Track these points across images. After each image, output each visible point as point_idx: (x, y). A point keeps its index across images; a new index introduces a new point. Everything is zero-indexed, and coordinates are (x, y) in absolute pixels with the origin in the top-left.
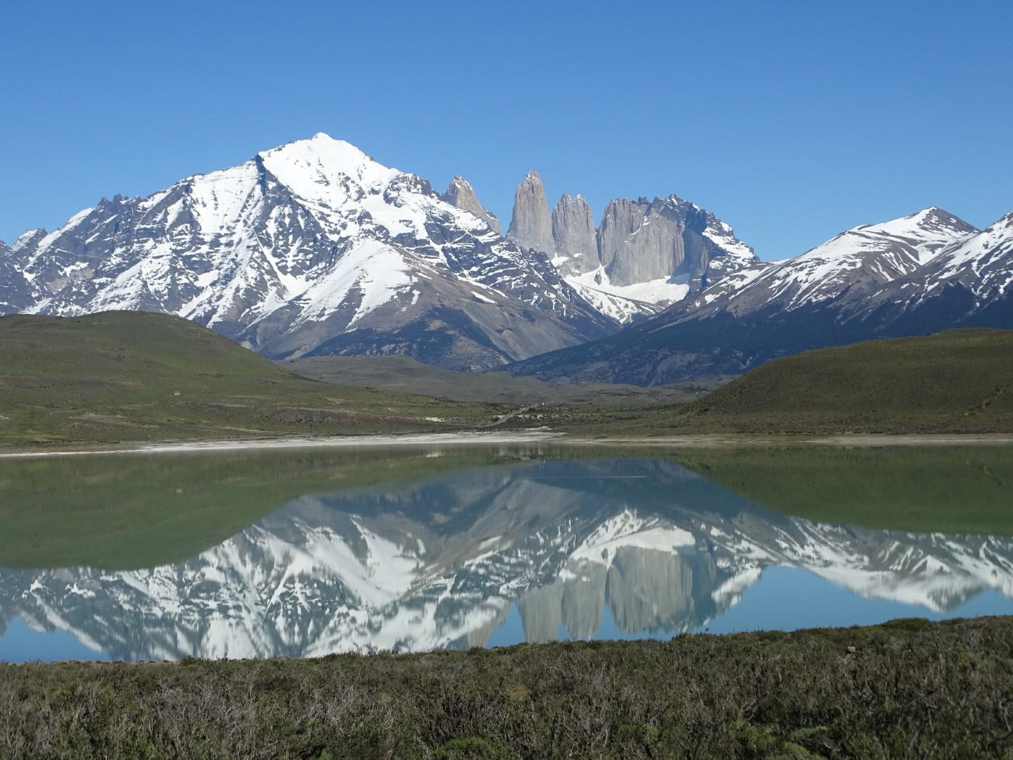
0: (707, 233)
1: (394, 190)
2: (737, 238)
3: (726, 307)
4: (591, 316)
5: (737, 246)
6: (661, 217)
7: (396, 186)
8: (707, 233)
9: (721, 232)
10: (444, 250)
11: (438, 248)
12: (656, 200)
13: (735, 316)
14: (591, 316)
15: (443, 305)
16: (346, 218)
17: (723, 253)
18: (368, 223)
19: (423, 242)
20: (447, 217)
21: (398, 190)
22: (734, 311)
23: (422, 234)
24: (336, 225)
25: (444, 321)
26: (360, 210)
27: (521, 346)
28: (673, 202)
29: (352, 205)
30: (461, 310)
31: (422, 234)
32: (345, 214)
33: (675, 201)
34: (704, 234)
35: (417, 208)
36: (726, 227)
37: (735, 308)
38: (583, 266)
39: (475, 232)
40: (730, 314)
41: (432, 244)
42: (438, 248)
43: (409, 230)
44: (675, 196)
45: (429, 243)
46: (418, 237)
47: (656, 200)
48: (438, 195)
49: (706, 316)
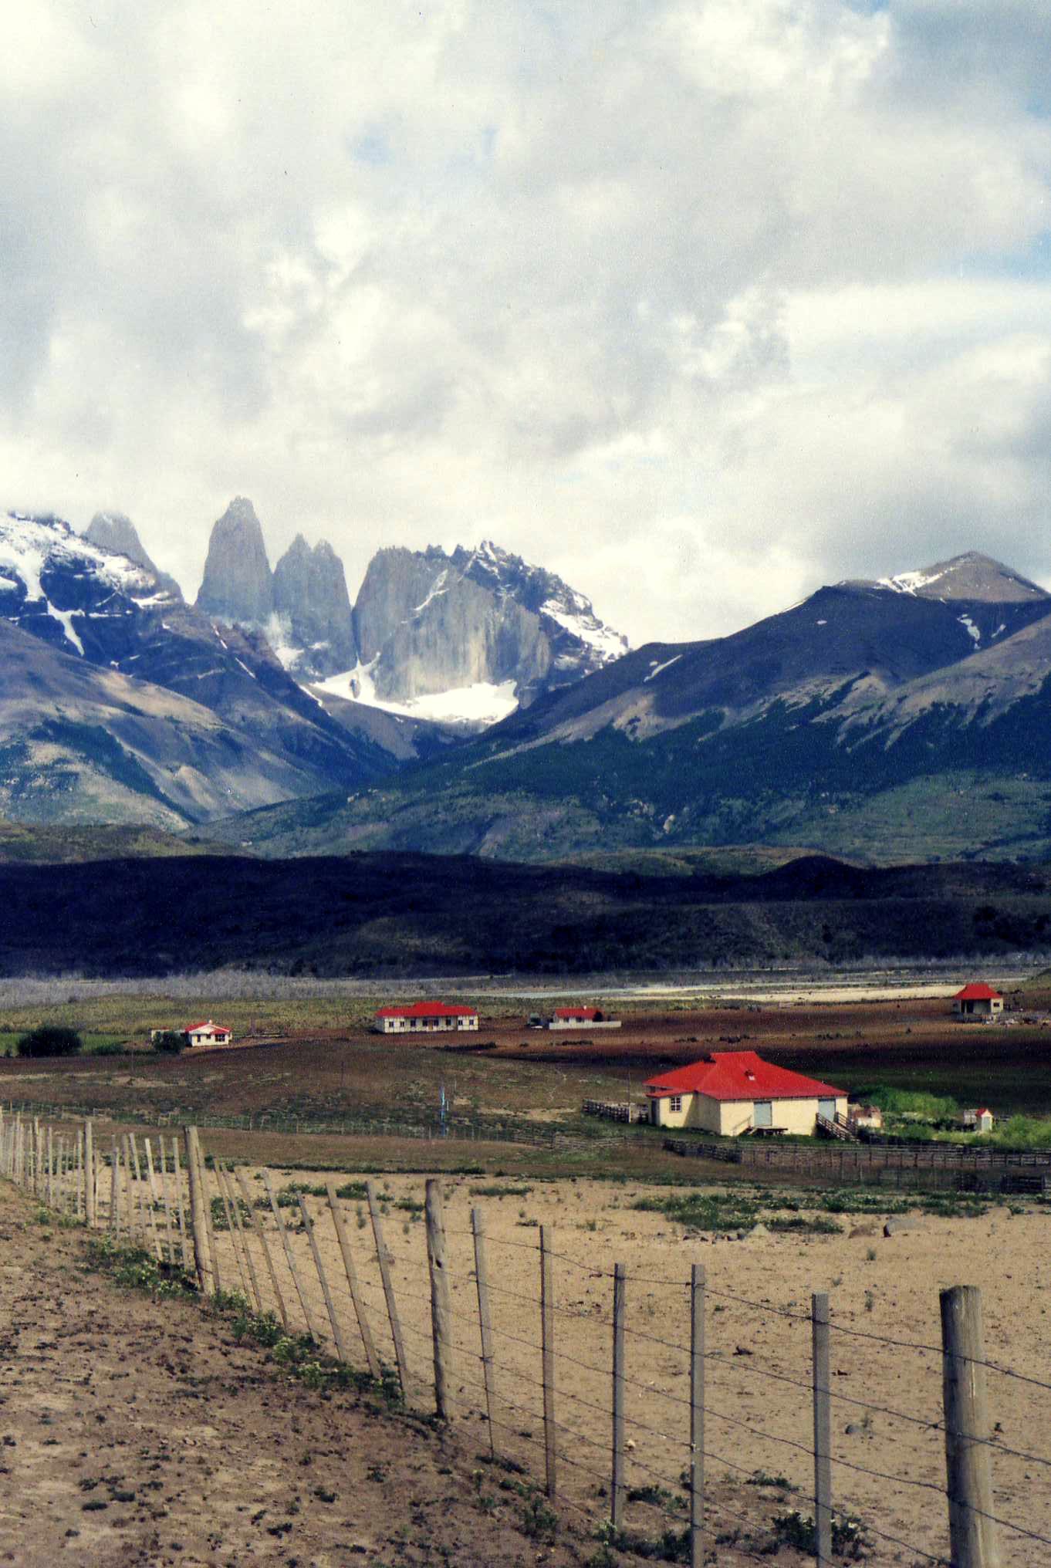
0: (551, 608)
2: (598, 617)
3: (613, 721)
4: (343, 745)
5: (598, 632)
6: (466, 581)
8: (551, 608)
9: (571, 610)
10: (75, 621)
11: (63, 616)
12: (459, 552)
13: (631, 738)
14: (343, 745)
15: (62, 718)
17: (577, 642)
19: (41, 606)
20: (79, 565)
22: (630, 728)
23: (35, 593)
25: (66, 744)
27: (212, 796)
28: (487, 555)
30: (100, 727)
31: (35, 593)
33: (490, 552)
34: (542, 610)
35: (24, 544)
36: (580, 603)
37: (631, 722)
38: (328, 665)
39: (132, 590)
40: (620, 735)
41: (52, 611)
42: (63, 616)
43: (11, 585)
44: (491, 544)
45: (45, 609)
46: (27, 599)
47: (459, 552)
48: (66, 526)
49: (571, 739)
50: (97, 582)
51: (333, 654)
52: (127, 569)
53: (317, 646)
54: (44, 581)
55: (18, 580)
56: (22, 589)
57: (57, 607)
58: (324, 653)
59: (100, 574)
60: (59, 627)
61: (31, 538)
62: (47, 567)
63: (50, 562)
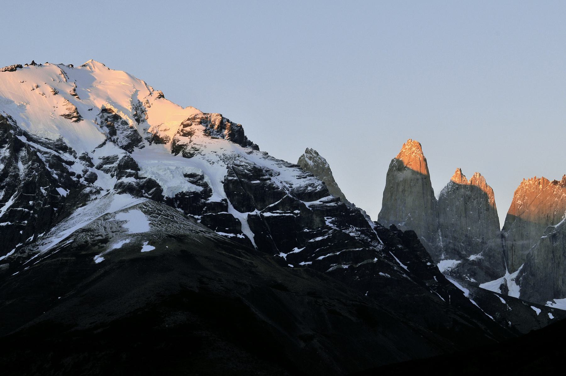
1: (185, 135)
7: (188, 129)
10: (251, 219)
11: (242, 217)
16: (99, 167)
18: (130, 175)
19: (221, 206)
21: (189, 134)
23: (218, 195)
24: (79, 177)
26: (121, 156)
29: (111, 150)
31: (218, 195)
32: (97, 162)
35: (214, 158)
42: (242, 217)
45: (226, 208)
50: (271, 187)
51: (487, 264)
52: (299, 177)
53: (472, 258)
54: (227, 184)
55: (205, 185)
56: (207, 192)
57: (235, 208)
58: (478, 263)
59: (276, 182)
60: (238, 223)
61: (220, 153)
62: (230, 174)
63: (232, 171)
